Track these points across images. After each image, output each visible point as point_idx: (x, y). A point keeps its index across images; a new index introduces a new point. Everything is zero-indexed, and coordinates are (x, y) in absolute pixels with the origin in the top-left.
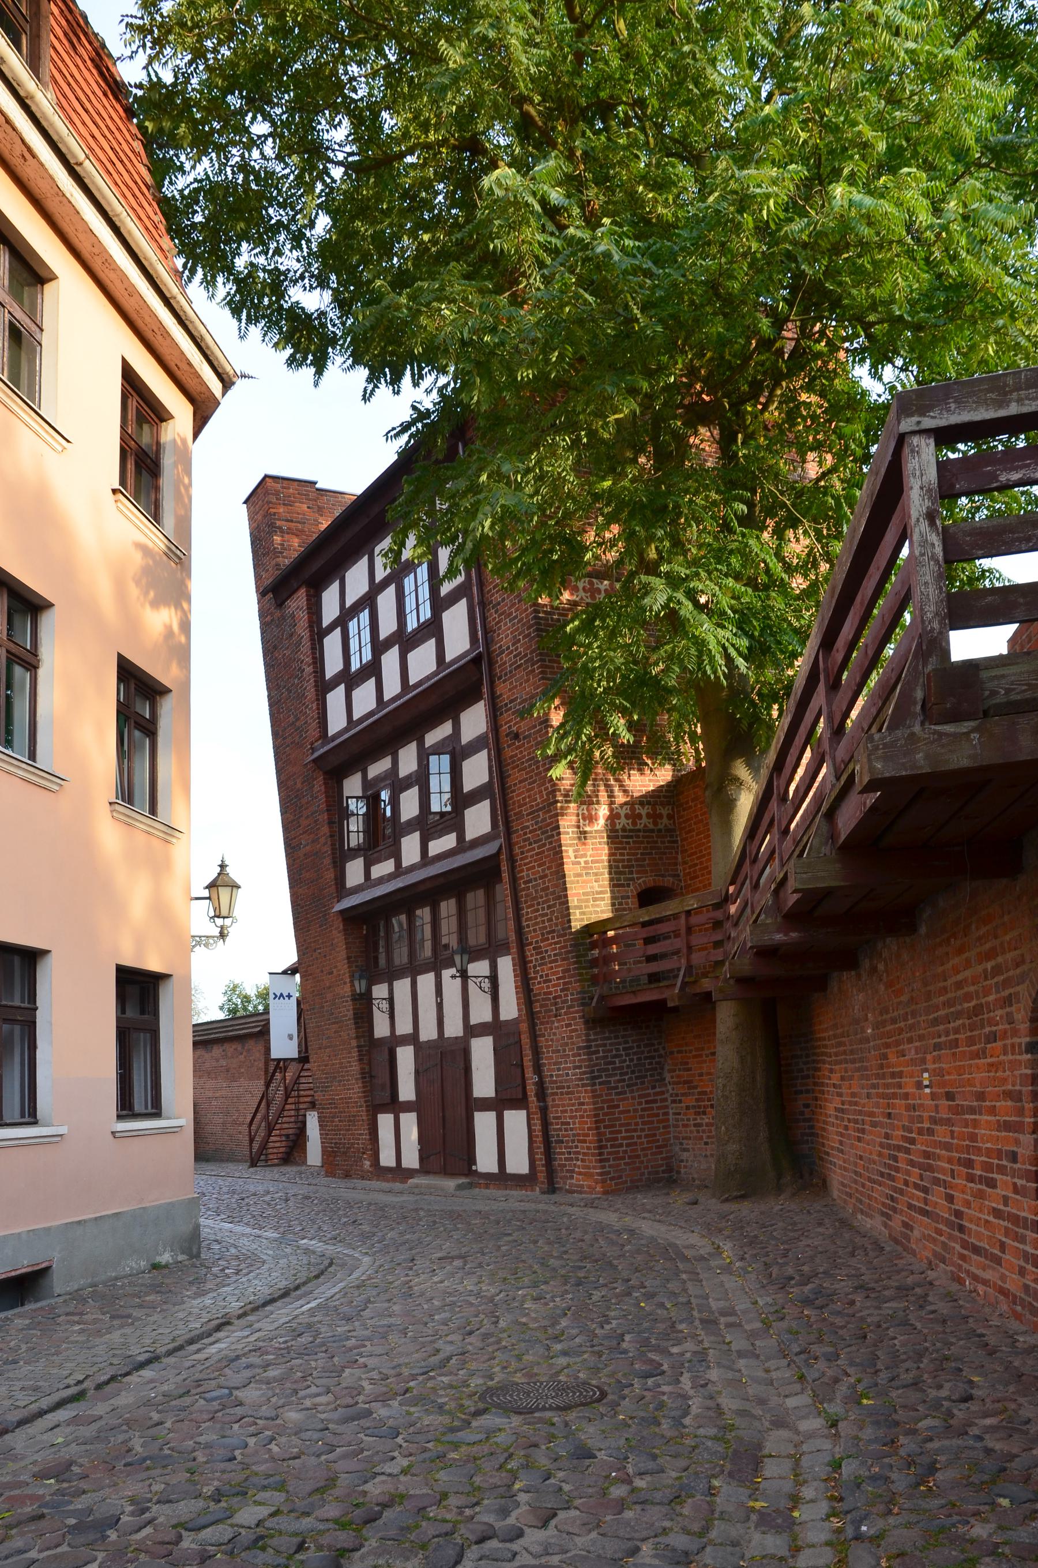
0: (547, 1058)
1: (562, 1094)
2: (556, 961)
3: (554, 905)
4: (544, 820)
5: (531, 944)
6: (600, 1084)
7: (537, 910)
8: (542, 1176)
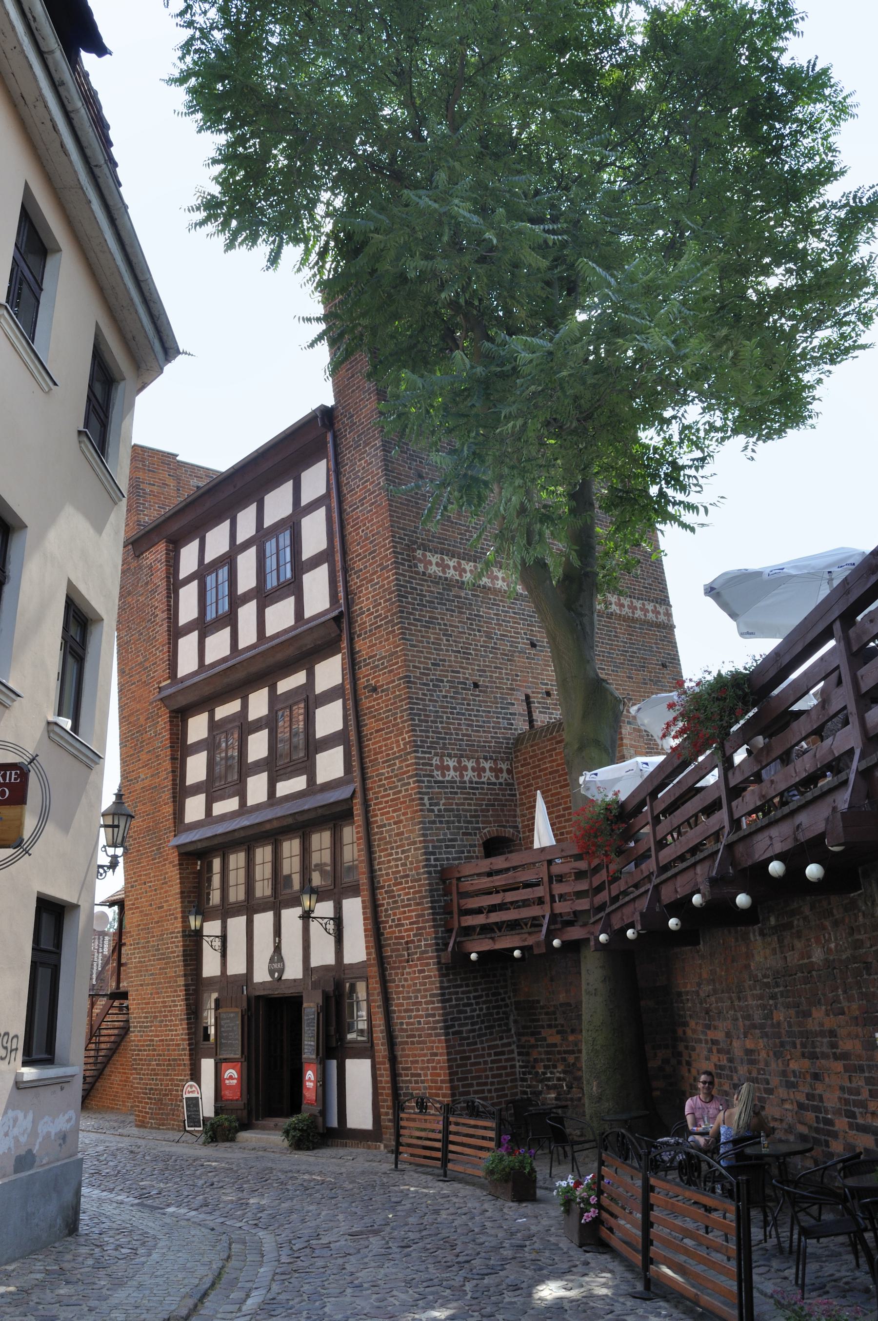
0: (398, 1005)
1: (413, 1043)
2: (409, 905)
3: (409, 850)
4: (401, 768)
5: (383, 887)
6: (454, 1033)
7: (391, 855)
8: (389, 1135)
